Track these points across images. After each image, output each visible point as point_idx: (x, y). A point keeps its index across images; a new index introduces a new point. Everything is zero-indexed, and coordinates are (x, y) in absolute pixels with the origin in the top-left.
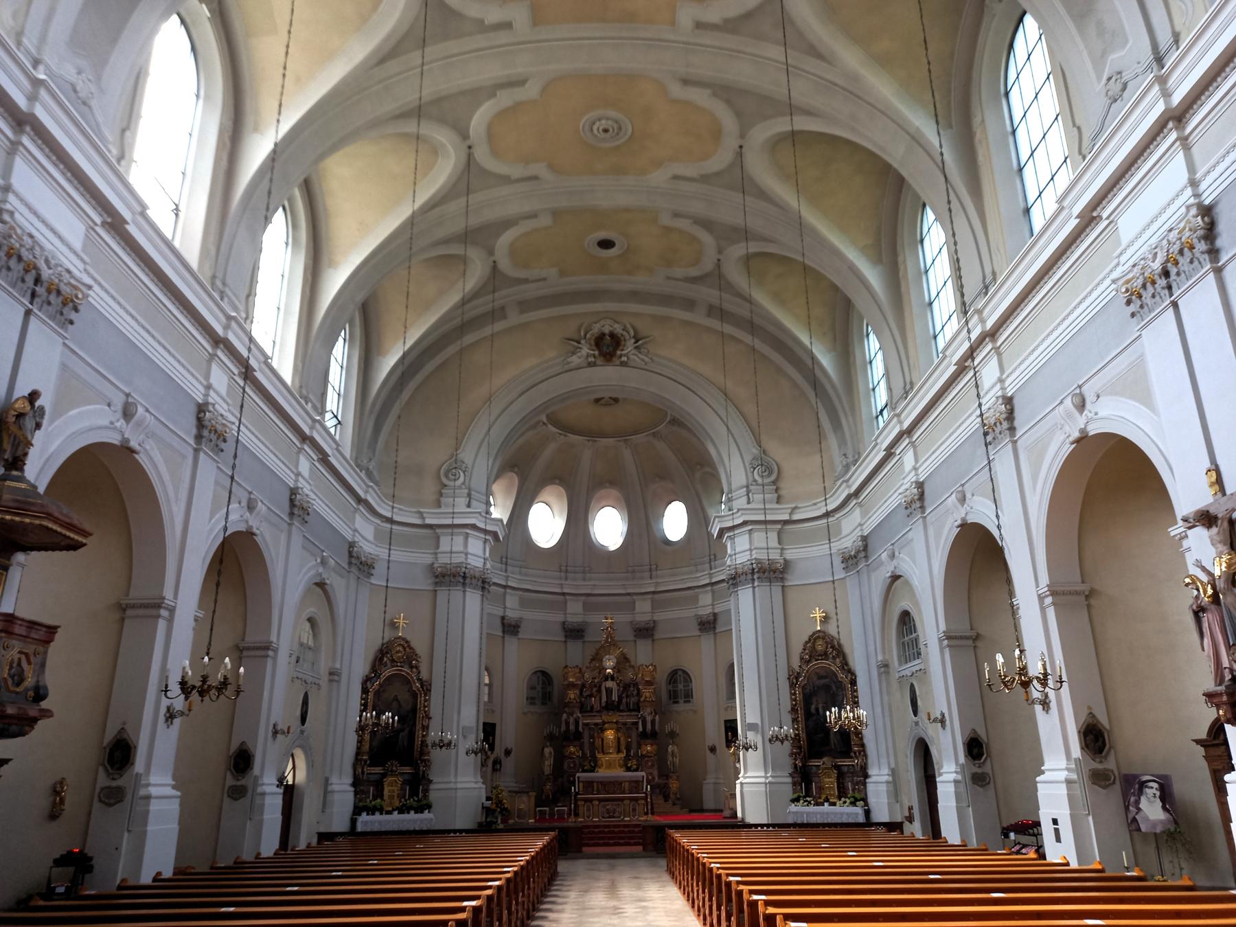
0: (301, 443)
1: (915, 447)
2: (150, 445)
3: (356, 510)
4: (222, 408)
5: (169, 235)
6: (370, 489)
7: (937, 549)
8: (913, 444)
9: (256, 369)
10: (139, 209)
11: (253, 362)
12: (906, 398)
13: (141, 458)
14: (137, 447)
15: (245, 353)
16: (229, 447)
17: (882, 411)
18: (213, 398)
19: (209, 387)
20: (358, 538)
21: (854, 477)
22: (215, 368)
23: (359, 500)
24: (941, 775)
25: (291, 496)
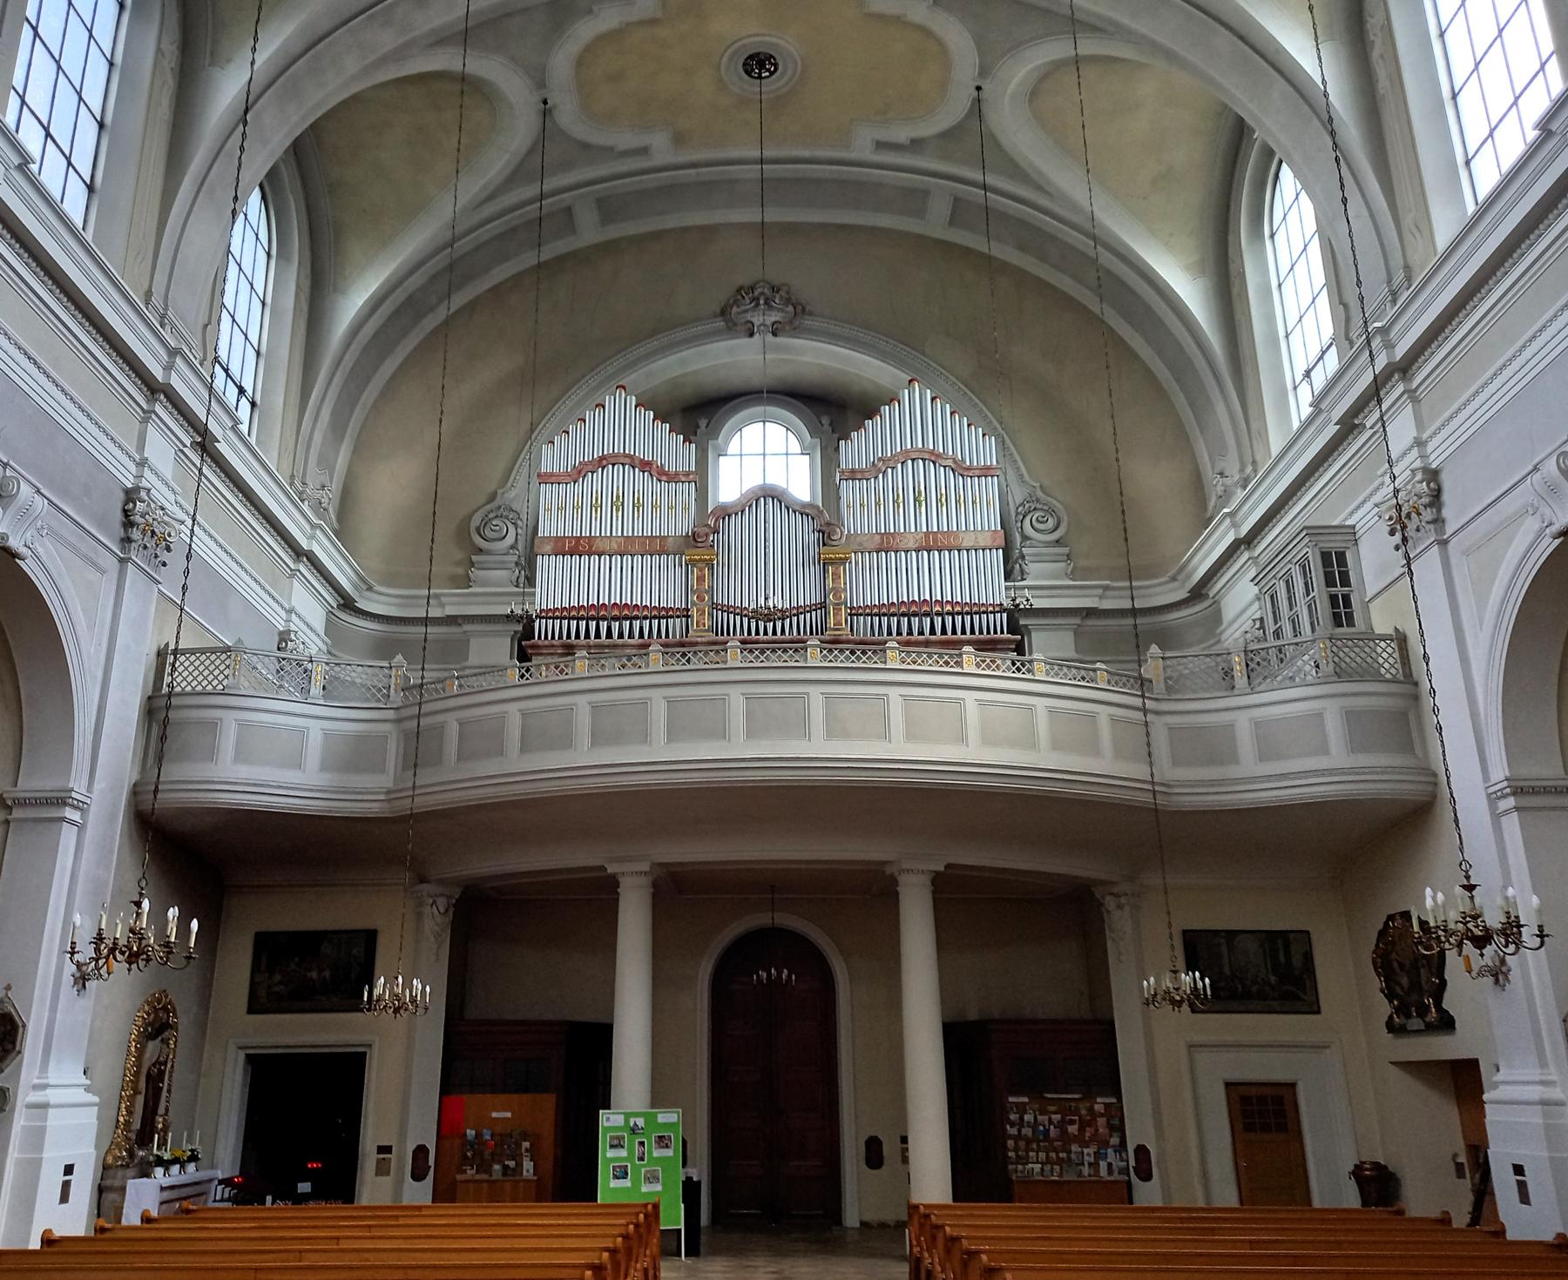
0: (148, 402)
1: (1415, 400)
2: (45, 548)
3: (293, 573)
4: (161, 495)
5: (56, 194)
6: (318, 532)
7: (1481, 605)
8: (1412, 395)
9: (220, 440)
10: (17, 161)
11: (213, 427)
12: (1394, 301)
13: (28, 566)
14: (23, 550)
15: (201, 413)
16: (176, 560)
17: (1308, 374)
18: (149, 479)
19: (142, 463)
20: (294, 625)
21: (1245, 508)
22: (152, 432)
23: (298, 553)
24: (1495, 1085)
25: (126, 503)
